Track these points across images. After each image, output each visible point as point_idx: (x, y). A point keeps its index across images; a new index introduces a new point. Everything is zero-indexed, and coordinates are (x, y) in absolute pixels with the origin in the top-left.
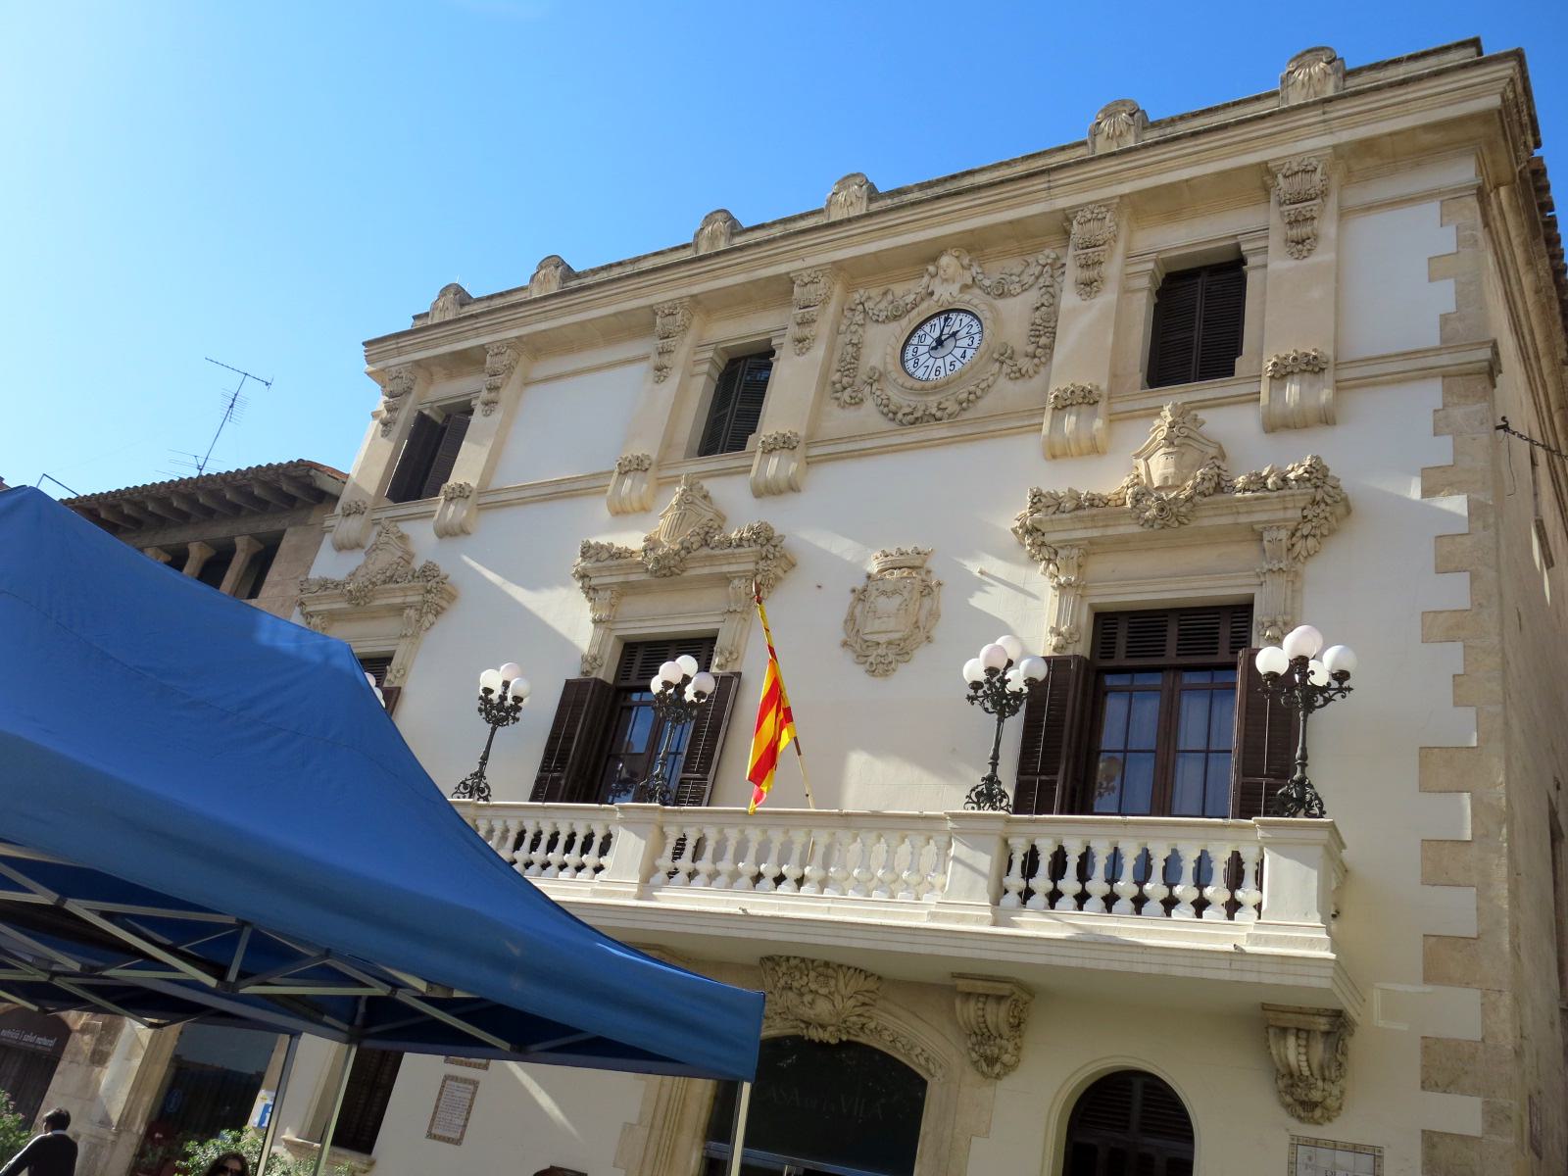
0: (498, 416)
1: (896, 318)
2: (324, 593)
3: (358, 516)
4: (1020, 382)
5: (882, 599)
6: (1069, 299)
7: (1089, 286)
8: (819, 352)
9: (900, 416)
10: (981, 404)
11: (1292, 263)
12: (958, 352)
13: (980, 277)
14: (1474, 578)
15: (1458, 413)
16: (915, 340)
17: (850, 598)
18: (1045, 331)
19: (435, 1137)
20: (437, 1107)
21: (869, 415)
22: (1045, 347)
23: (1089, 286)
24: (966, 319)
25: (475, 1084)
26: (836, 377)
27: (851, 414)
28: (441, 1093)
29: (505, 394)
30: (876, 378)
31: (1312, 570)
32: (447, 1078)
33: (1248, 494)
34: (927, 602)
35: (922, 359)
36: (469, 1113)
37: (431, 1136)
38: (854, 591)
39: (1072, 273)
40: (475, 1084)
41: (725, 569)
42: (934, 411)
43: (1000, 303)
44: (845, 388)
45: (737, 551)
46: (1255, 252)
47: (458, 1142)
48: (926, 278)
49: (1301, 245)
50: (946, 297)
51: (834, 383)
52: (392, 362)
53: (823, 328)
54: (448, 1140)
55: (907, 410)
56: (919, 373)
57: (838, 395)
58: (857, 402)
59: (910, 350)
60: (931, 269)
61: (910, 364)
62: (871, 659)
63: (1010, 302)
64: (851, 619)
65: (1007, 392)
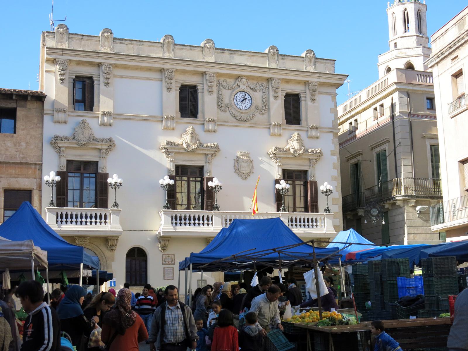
2: (67, 141)
3: (63, 113)
4: (262, 115)
6: (272, 99)
8: (215, 96)
9: (238, 118)
11: (311, 104)
12: (247, 104)
14: (338, 171)
16: (235, 97)
19: (166, 280)
20: (164, 274)
21: (227, 115)
23: (276, 97)
25: (173, 268)
28: (164, 271)
32: (164, 268)
33: (311, 153)
34: (251, 164)
35: (239, 103)
36: (173, 273)
37: (164, 279)
41: (206, 152)
42: (246, 119)
43: (254, 93)
45: (211, 149)
46: (303, 97)
47: (173, 279)
50: (243, 88)
54: (171, 280)
56: (238, 107)
57: (221, 108)
58: (225, 111)
59: (235, 99)
61: (236, 103)
65: (259, 118)
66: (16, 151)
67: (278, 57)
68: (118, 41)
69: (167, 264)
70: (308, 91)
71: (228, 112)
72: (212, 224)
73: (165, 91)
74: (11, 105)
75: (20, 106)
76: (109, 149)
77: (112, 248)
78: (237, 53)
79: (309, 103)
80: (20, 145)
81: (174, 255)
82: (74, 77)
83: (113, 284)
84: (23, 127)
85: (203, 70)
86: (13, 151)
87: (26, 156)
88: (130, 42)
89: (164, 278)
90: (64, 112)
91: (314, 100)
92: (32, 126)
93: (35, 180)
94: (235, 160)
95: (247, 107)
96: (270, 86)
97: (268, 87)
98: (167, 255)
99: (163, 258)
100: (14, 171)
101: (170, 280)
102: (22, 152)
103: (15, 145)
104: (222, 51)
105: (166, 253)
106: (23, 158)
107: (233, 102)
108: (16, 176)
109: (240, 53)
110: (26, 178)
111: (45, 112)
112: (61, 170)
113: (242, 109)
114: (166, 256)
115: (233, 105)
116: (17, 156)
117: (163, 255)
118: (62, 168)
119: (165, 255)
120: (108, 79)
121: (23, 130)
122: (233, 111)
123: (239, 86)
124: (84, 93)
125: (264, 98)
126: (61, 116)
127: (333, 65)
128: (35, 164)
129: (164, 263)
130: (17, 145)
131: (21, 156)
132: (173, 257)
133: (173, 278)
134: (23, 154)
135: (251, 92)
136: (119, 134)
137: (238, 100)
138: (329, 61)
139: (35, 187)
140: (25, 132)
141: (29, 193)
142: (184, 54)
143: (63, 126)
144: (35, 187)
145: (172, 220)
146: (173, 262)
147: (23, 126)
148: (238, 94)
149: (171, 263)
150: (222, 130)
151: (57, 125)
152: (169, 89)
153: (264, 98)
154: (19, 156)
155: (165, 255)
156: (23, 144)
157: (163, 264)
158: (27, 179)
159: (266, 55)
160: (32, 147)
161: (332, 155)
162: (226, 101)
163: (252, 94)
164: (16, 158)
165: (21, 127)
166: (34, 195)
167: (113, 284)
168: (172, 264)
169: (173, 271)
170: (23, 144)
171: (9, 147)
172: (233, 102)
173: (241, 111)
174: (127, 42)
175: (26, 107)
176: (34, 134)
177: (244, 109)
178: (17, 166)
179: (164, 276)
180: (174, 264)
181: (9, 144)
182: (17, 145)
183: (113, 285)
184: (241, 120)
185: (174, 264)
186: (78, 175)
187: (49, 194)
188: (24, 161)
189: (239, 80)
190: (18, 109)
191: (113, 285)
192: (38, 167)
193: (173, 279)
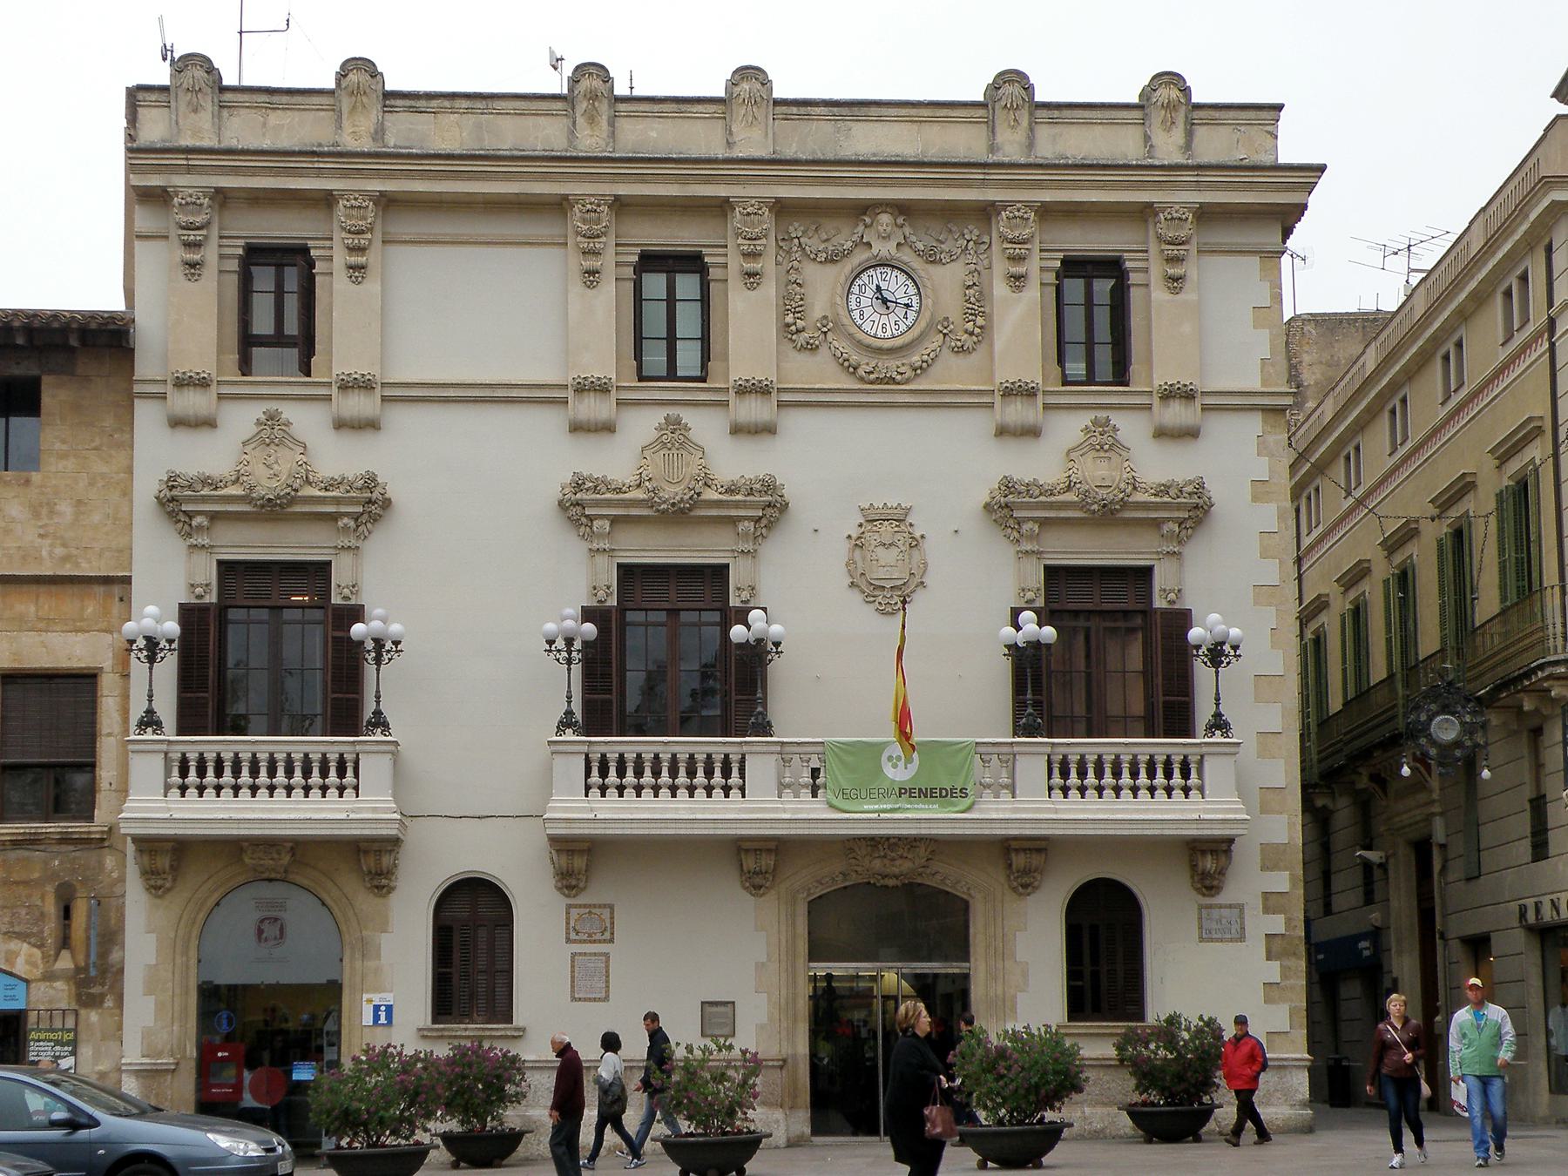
0: (372, 286)
1: (833, 261)
5: (880, 550)
6: (1000, 289)
7: (1017, 280)
8: (769, 290)
9: (861, 372)
10: (932, 370)
11: (1167, 296)
13: (914, 238)
15: (1271, 439)
16: (855, 289)
17: (847, 545)
18: (977, 306)
20: (573, 977)
22: (981, 327)
23: (1017, 280)
24: (902, 278)
25: (607, 955)
26: (789, 319)
27: (804, 358)
28: (573, 967)
29: (372, 258)
30: (829, 326)
31: (1189, 551)
32: (574, 955)
34: (915, 552)
35: (868, 312)
37: (574, 999)
38: (849, 537)
39: (1000, 267)
40: (607, 955)
41: (733, 513)
42: (894, 375)
43: (931, 268)
44: (798, 331)
47: (606, 999)
48: (861, 228)
49: (1175, 283)
50: (884, 253)
51: (788, 325)
52: (179, 180)
53: (767, 265)
54: (600, 1000)
55: (869, 369)
59: (853, 298)
60: (868, 220)
61: (856, 314)
62: (879, 599)
63: (936, 271)
64: (850, 563)
66: (41, 536)
67: (1031, 114)
68: (399, 102)
69: (585, 941)
70: (1154, 248)
71: (824, 351)
72: (742, 789)
73: (576, 288)
74: (19, 369)
75: (50, 372)
76: (366, 516)
77: (380, 880)
78: (864, 110)
79: (1159, 294)
80: (52, 512)
81: (611, 907)
82: (241, 252)
83: (383, 1015)
84: (64, 447)
85: (721, 191)
86: (30, 536)
87: (75, 552)
88: (447, 103)
89: (573, 991)
90: (203, 384)
91: (1175, 279)
92: (97, 442)
93: (109, 637)
94: (849, 537)
95: (903, 328)
96: (995, 235)
97: (986, 239)
98: (585, 906)
99: (568, 919)
100: (32, 609)
101: (595, 1000)
102: (62, 537)
103: (36, 515)
104: (803, 110)
105: (581, 899)
106: (66, 559)
107: (843, 312)
108: (41, 625)
109: (874, 111)
110: (77, 631)
111: (137, 388)
112: (194, 601)
113: (880, 333)
114: (583, 911)
115: (846, 321)
116: (44, 553)
117: (569, 907)
118: (199, 590)
119: (576, 906)
120: (360, 250)
121: (64, 456)
122: (843, 346)
123: (869, 245)
124: (277, 306)
125: (969, 287)
126: (193, 402)
127: (1269, 128)
128: (107, 581)
129: (573, 936)
130: (44, 511)
131: (59, 551)
132: (606, 913)
133: (607, 992)
134: (64, 545)
135: (916, 264)
136: (405, 456)
137: (865, 302)
138: (1251, 114)
139: (107, 664)
140: (70, 464)
141: (86, 680)
142: (654, 134)
143: (202, 438)
144: (107, 664)
145: (588, 774)
146: (607, 935)
147: (64, 442)
148: (865, 277)
149: (598, 937)
150: (797, 423)
151: (184, 437)
152: (591, 276)
153: (969, 287)
154: (50, 554)
155: (576, 906)
156: (66, 508)
157: (568, 940)
158: (80, 636)
159: (982, 112)
160: (96, 518)
161: (1255, 499)
162: (818, 307)
163: (923, 274)
164: (39, 559)
165: (58, 446)
166: (105, 692)
167: (383, 1015)
168: (604, 941)
169: (607, 967)
170: (66, 508)
171: (13, 520)
172: (843, 312)
173: (879, 343)
174: (434, 103)
175: (73, 374)
176: (104, 469)
177: (889, 334)
178: (43, 589)
179: (572, 987)
180: (611, 941)
181: (15, 510)
182: (44, 511)
183: (383, 1020)
184: (872, 376)
185: (611, 941)
186: (264, 614)
187: (160, 685)
188: (67, 570)
189: (868, 220)
190: (46, 381)
191: (383, 1020)
192: (117, 590)
193: (606, 999)
